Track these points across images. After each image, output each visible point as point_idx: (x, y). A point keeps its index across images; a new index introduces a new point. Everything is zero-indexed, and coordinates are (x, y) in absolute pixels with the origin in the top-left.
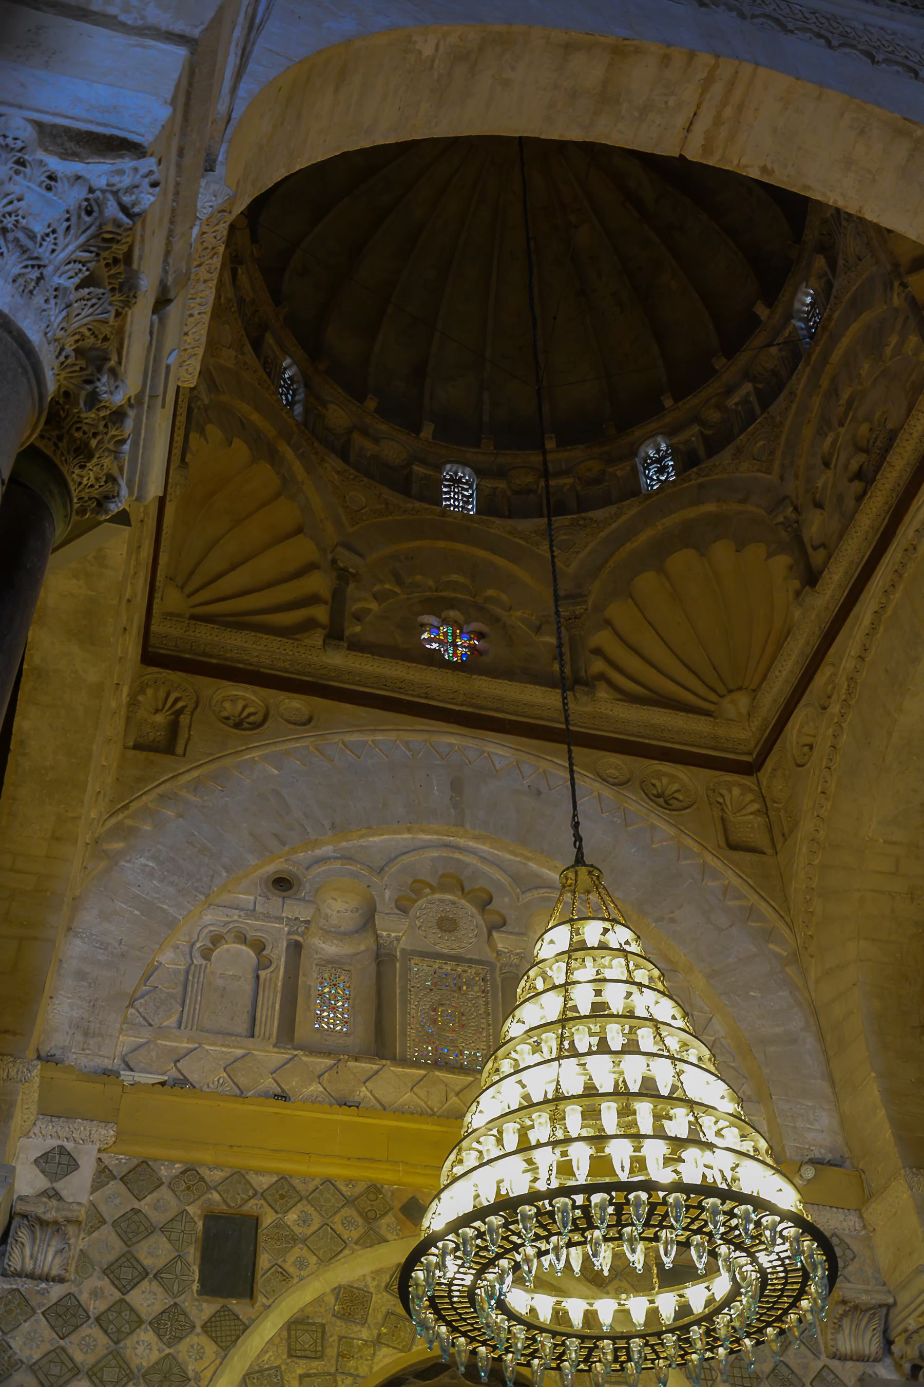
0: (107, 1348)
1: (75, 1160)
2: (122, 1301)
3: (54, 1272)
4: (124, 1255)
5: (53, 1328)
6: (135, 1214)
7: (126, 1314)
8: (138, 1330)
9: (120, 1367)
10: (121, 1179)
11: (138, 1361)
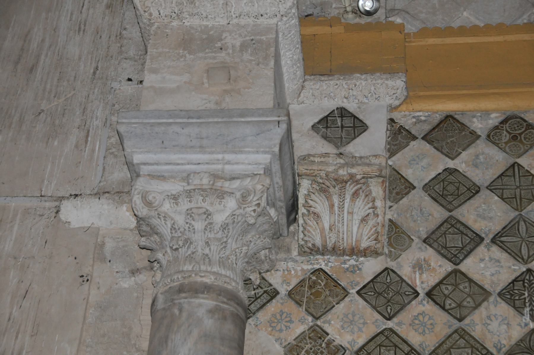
0: (450, 326)
1: (361, 121)
2: (456, 272)
3: (364, 244)
4: (446, 221)
5: (374, 308)
6: (451, 174)
7: (464, 286)
8: (485, 303)
9: (472, 347)
10: (423, 138)
11: (495, 339)
